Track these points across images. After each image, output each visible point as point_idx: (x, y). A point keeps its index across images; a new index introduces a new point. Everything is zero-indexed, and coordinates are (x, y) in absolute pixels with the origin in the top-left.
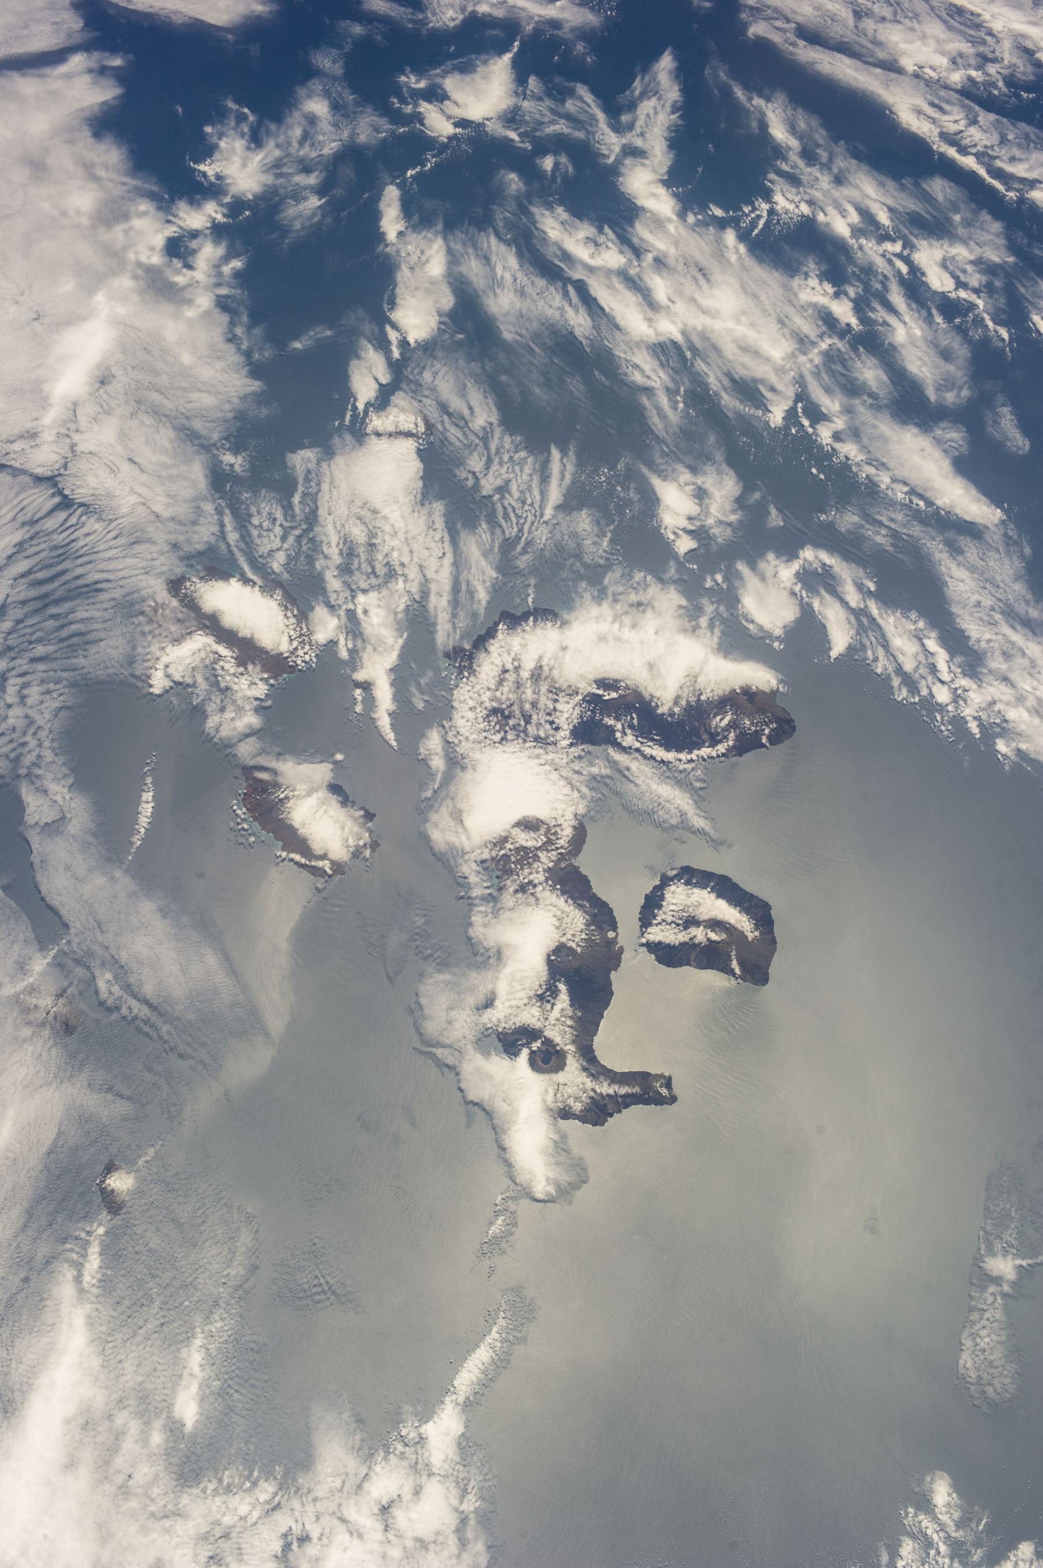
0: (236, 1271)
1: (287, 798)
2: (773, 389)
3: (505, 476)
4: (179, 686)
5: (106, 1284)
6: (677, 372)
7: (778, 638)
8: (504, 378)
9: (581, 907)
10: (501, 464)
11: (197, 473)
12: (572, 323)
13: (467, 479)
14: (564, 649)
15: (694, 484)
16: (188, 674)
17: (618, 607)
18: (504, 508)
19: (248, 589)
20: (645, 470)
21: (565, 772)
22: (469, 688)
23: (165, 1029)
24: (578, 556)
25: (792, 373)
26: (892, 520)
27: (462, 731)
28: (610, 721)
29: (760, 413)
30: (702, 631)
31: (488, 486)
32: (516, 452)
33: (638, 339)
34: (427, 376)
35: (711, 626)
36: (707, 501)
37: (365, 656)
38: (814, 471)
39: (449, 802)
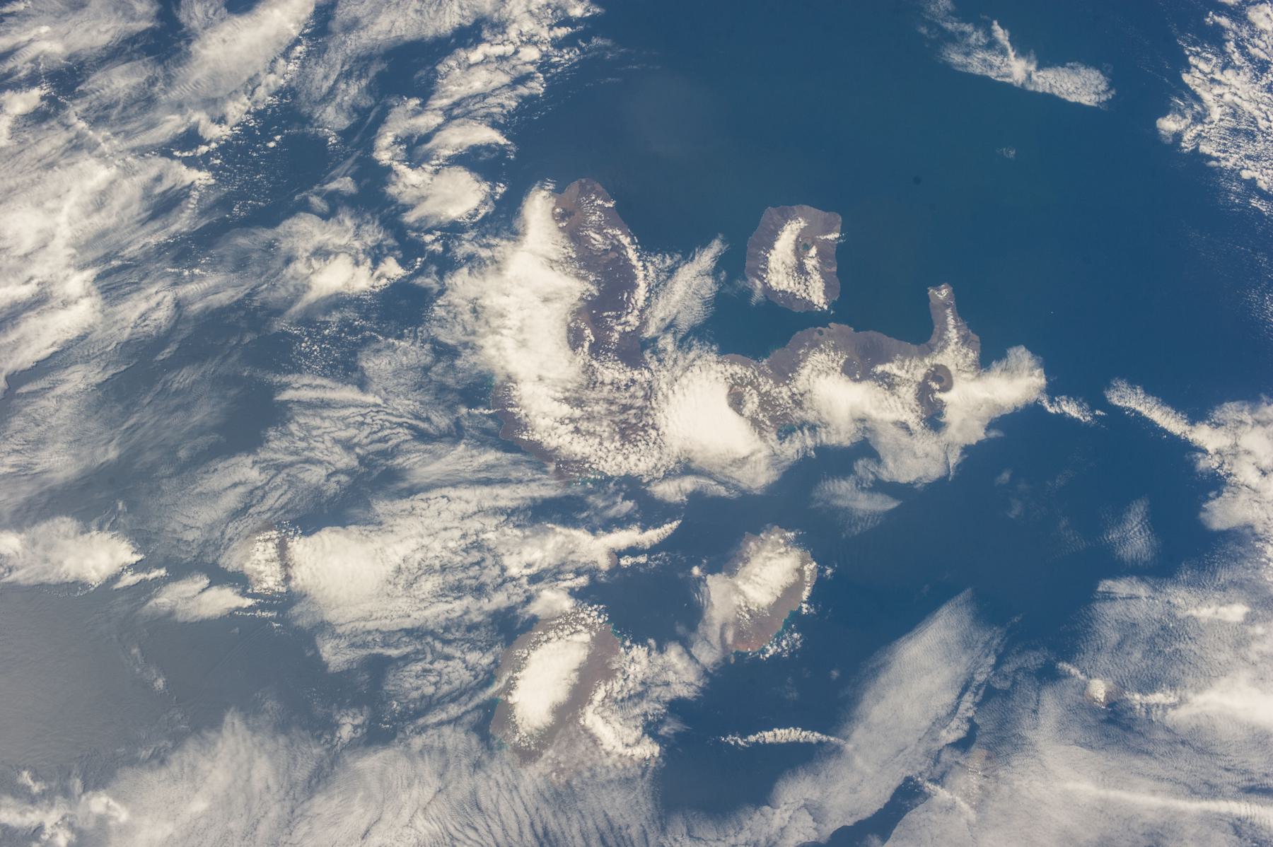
0: (1142, 591)
1: (749, 611)
2: (159, 179)
3: (329, 445)
4: (651, 729)
5: (1173, 685)
6: (146, 275)
7: (492, 188)
8: (183, 454)
9: (806, 355)
10: (313, 449)
11: (370, 763)
12: (82, 386)
13: (338, 482)
14: (540, 379)
15: (308, 259)
16: (633, 723)
17: (482, 330)
18: (371, 443)
19: (518, 683)
20: (298, 307)
21: (678, 372)
22: (603, 462)
23: (980, 678)
24: (426, 369)
25: (129, 159)
26: (326, 77)
27: (651, 465)
28: (617, 335)
29: (195, 194)
30: (496, 254)
31: (346, 460)
32: (292, 434)
33: (100, 316)
34: (190, 536)
35: (488, 246)
36: (330, 247)
37: (583, 560)
38: (272, 145)
39: (727, 471)
